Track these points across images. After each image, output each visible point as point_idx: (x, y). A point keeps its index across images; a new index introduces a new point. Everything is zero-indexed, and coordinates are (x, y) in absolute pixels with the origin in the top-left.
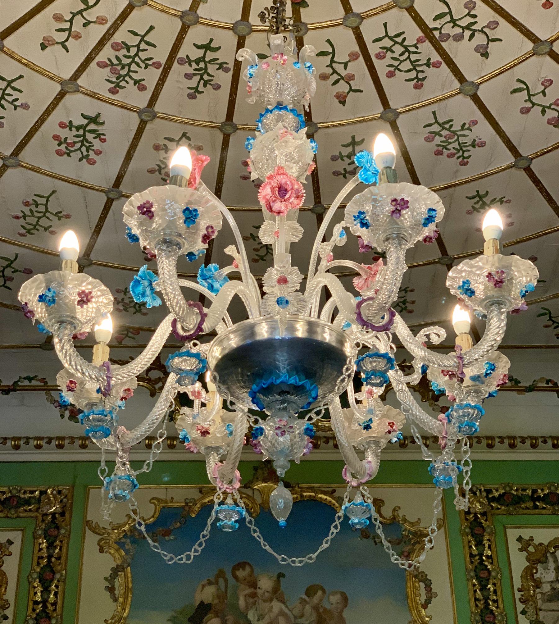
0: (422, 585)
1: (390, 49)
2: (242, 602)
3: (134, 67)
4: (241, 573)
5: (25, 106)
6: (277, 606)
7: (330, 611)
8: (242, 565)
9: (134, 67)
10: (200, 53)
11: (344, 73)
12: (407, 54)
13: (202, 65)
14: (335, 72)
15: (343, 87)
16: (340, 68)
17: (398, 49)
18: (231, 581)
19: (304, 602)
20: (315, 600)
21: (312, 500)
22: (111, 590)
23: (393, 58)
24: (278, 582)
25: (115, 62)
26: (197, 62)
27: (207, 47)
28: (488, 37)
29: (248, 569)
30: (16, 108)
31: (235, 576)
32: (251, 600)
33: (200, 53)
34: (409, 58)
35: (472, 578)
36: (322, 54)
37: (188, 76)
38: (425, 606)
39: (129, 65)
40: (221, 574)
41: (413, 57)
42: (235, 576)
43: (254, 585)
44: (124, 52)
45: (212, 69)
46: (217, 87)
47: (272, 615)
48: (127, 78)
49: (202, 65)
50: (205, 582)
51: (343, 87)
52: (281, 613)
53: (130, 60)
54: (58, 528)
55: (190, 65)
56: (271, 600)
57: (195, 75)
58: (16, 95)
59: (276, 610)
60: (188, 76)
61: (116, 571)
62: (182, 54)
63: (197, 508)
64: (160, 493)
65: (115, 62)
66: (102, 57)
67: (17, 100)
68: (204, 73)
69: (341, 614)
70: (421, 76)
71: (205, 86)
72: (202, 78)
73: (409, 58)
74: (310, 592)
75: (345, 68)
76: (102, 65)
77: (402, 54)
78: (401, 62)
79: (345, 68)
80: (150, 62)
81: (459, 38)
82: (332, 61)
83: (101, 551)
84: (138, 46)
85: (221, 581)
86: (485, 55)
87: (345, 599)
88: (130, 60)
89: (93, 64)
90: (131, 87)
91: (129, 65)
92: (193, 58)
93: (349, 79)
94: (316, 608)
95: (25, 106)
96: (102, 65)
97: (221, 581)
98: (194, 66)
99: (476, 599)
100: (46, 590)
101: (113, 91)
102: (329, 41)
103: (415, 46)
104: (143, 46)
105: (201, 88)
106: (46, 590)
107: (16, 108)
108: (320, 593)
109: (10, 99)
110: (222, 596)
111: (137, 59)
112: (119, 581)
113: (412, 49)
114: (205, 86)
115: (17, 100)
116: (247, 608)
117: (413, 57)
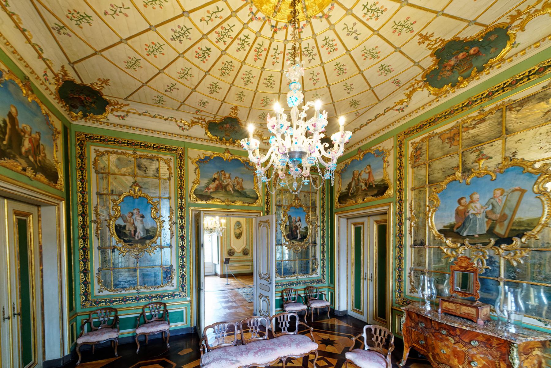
3: (225, 36)
5: (190, 39)
9: (225, 36)
10: (244, 38)
21: (237, 159)
25: (220, 33)
26: (243, 40)
27: (247, 37)
30: (187, 38)
33: (244, 38)
37: (239, 44)
39: (224, 35)
44: (224, 30)
45: (246, 44)
53: (224, 34)
58: (188, 34)
60: (239, 44)
62: (239, 37)
63: (213, 157)
65: (220, 33)
66: (217, 30)
67: (188, 36)
76: (216, 33)
81: (306, 55)
88: (224, 34)
89: (214, 32)
91: (224, 35)
92: (242, 39)
94: (237, 181)
95: (190, 39)
96: (216, 33)
98: (241, 42)
101: (217, 42)
104: (230, 30)
107: (187, 38)
109: (186, 35)
115: (188, 36)
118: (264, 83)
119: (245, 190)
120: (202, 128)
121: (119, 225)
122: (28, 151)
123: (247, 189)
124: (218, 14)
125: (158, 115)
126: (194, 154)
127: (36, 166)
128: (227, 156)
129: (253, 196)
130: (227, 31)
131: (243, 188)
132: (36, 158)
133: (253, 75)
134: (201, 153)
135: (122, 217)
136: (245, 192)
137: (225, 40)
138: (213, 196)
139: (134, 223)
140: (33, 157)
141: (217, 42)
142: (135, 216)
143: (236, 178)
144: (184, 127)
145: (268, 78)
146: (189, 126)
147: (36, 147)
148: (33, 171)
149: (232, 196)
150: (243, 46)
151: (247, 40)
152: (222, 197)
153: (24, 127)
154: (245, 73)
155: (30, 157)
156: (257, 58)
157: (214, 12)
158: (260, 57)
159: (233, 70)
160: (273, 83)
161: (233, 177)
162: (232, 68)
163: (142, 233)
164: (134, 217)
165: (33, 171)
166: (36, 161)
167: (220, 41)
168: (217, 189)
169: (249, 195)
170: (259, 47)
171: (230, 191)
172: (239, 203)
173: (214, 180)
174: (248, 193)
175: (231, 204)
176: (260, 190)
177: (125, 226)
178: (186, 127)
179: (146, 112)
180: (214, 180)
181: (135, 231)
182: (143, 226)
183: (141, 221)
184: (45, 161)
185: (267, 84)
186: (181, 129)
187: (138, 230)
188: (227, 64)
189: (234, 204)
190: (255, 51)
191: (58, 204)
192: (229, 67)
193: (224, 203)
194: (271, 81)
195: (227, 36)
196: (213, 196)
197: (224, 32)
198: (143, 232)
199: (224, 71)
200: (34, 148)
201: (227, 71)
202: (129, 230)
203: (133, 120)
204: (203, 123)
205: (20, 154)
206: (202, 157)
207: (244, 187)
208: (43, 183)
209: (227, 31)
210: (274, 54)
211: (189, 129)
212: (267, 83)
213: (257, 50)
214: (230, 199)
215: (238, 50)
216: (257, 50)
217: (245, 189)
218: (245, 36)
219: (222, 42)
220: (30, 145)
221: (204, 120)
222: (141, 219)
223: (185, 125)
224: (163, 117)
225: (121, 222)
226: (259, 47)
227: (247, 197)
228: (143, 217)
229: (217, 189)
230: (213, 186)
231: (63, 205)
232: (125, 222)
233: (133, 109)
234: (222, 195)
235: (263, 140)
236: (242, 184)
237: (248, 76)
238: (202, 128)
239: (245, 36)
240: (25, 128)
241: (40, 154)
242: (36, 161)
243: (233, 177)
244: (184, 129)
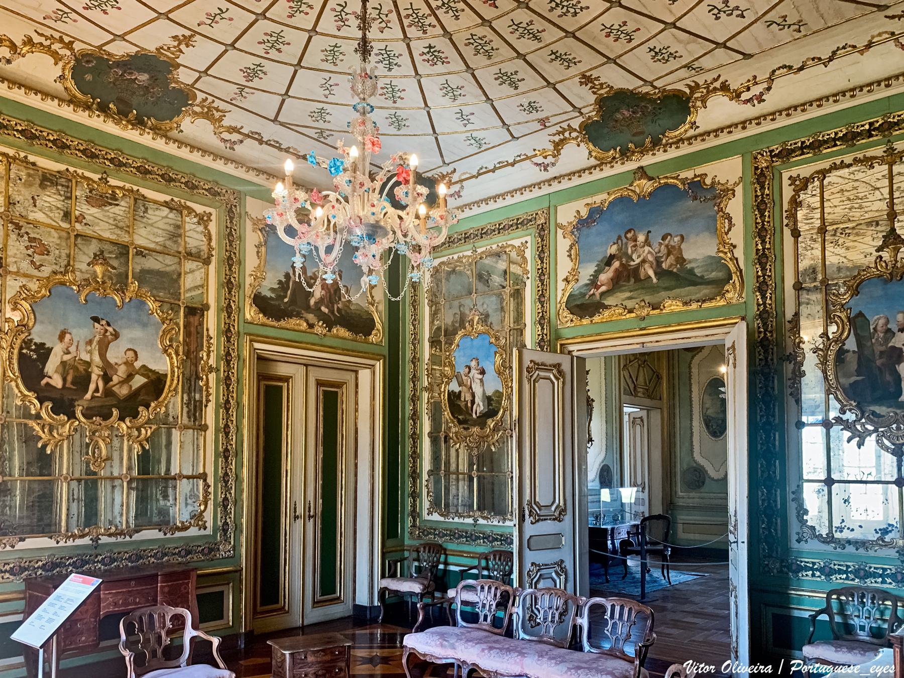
0: (726, 221)
2: (630, 251)
4: (629, 235)
6: (647, 249)
7: (674, 246)
8: (629, 231)
18: (625, 240)
19: (660, 244)
20: (667, 242)
22: (570, 256)
24: (648, 236)
29: (633, 232)
31: (626, 237)
32: (634, 249)
35: (755, 211)
38: (727, 234)
40: (619, 238)
42: (626, 237)
43: (636, 240)
47: (645, 254)
50: (612, 243)
52: (649, 252)
54: (544, 231)
56: (644, 246)
59: (646, 252)
61: (571, 247)
64: (589, 200)
69: (680, 247)
74: (664, 238)
83: (564, 237)
85: (620, 241)
87: (682, 237)
94: (667, 246)
97: (620, 241)
99: (757, 223)
100: (542, 262)
106: (542, 262)
108: (669, 237)
110: (620, 249)
112: (573, 252)
116: (632, 253)
119: (689, 266)
120: (579, 145)
121: (452, 391)
122: (321, 301)
123: (695, 260)
125: (499, 163)
126: (567, 214)
127: (332, 317)
128: (647, 186)
129: (713, 275)
131: (684, 260)
132: (333, 307)
134: (581, 207)
135: (458, 376)
136: (691, 271)
138: (608, 301)
139: (471, 387)
140: (327, 307)
142: (473, 371)
143: (664, 238)
144: (546, 161)
146: (554, 156)
147: (332, 292)
148: (325, 325)
149: (654, 289)
152: (630, 298)
153: (314, 274)
155: (323, 309)
161: (656, 239)
163: (481, 404)
164: (471, 375)
165: (325, 325)
166: (332, 312)
168: (616, 283)
169: (702, 277)
171: (650, 277)
172: (673, 306)
173: (609, 261)
174: (698, 272)
175: (652, 312)
176: (739, 253)
177: (460, 392)
178: (550, 159)
179: (481, 168)
180: (609, 261)
181: (473, 402)
182: (484, 390)
183: (481, 380)
184: (348, 307)
186: (542, 168)
187: (477, 400)
189: (657, 312)
191: (373, 366)
193: (633, 315)
196: (608, 301)
198: (483, 402)
200: (330, 296)
202: (465, 401)
203: (473, 190)
204: (574, 134)
205: (308, 308)
206: (584, 213)
207: (685, 257)
208: (344, 338)
211: (557, 161)
214: (648, 299)
217: (690, 262)
220: (323, 292)
221: (571, 129)
222: (480, 376)
223: (545, 157)
224: (507, 161)
225: (454, 387)
227: (694, 283)
228: (483, 372)
229: (616, 283)
230: (604, 277)
231: (379, 366)
232: (460, 386)
233: (464, 173)
234: (628, 294)
235: (738, 96)
236: (680, 250)
238: (579, 145)
240: (316, 273)
241: (340, 299)
242: (332, 312)
243: (656, 239)
244: (548, 165)
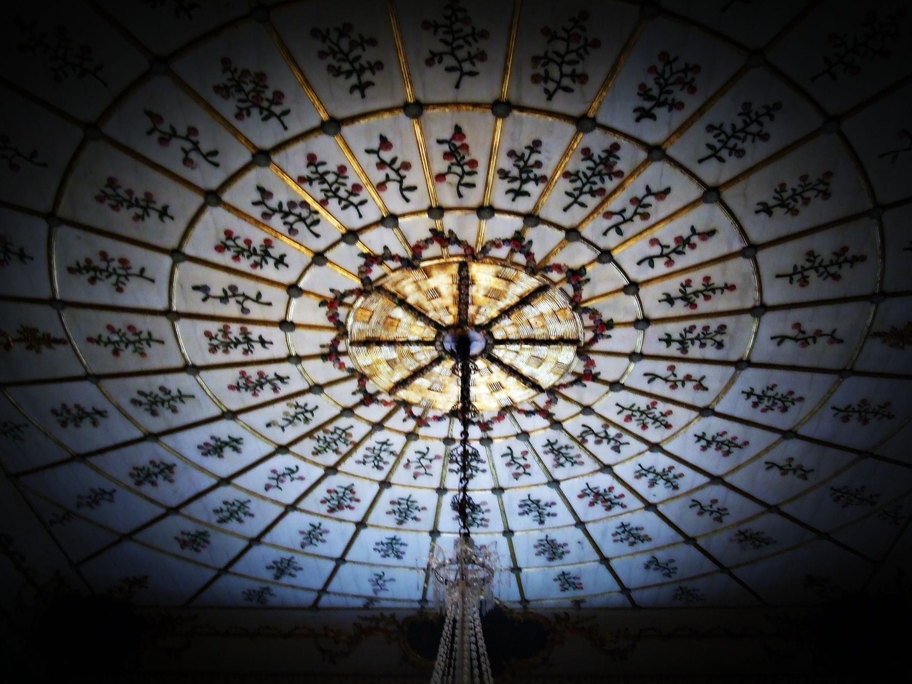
1: (351, 194)
9: (589, 173)
11: (388, 171)
12: (333, 188)
13: (524, 176)
14: (397, 171)
15: (387, 156)
16: (393, 175)
17: (342, 193)
23: (344, 185)
26: (528, 180)
27: (518, 193)
28: (267, 206)
34: (330, 186)
36: (413, 188)
37: (538, 164)
39: (593, 175)
41: (326, 186)
45: (515, 172)
46: (511, 154)
48: (598, 161)
49: (524, 176)
51: (387, 156)
55: (535, 175)
57: (532, 166)
60: (538, 164)
68: (523, 167)
70: (313, 168)
71: (523, 155)
72: (526, 163)
73: (330, 186)
75: (387, 176)
77: (338, 189)
78: (336, 182)
79: (387, 176)
80: (573, 178)
82: (401, 182)
84: (581, 193)
86: (261, 190)
90: (597, 152)
93: (381, 164)
98: (532, 175)
101: (615, 147)
102: (407, 200)
103: (328, 197)
105: (527, 152)
111: (584, 180)
113: (330, 194)
114: (523, 155)
117: (326, 186)
118: (373, 42)
124: (616, 219)
130: (586, 189)
133: (439, 69)
137: (590, 164)
141: (615, 147)
145: (367, 76)
150: (521, 164)
151: (516, 185)
154: (479, 66)
156: (458, 144)
157: (631, 219)
158: (446, 148)
159: (536, 60)
160: (330, 60)
162: (541, 71)
167: (603, 155)
170: (467, 179)
185: (353, 45)
188: (566, 82)
190: (473, 163)
192: (555, 73)
194: (346, 66)
195: (581, 175)
197: (595, 183)
199: (573, 46)
201: (561, 47)
209: (586, 189)
210: (402, 172)
212: (358, 52)
213: (467, 168)
215: (535, 146)
216: (467, 168)
218: (527, 194)
219: (597, 152)
226: (467, 179)
237: (462, 54)
239: (527, 194)
